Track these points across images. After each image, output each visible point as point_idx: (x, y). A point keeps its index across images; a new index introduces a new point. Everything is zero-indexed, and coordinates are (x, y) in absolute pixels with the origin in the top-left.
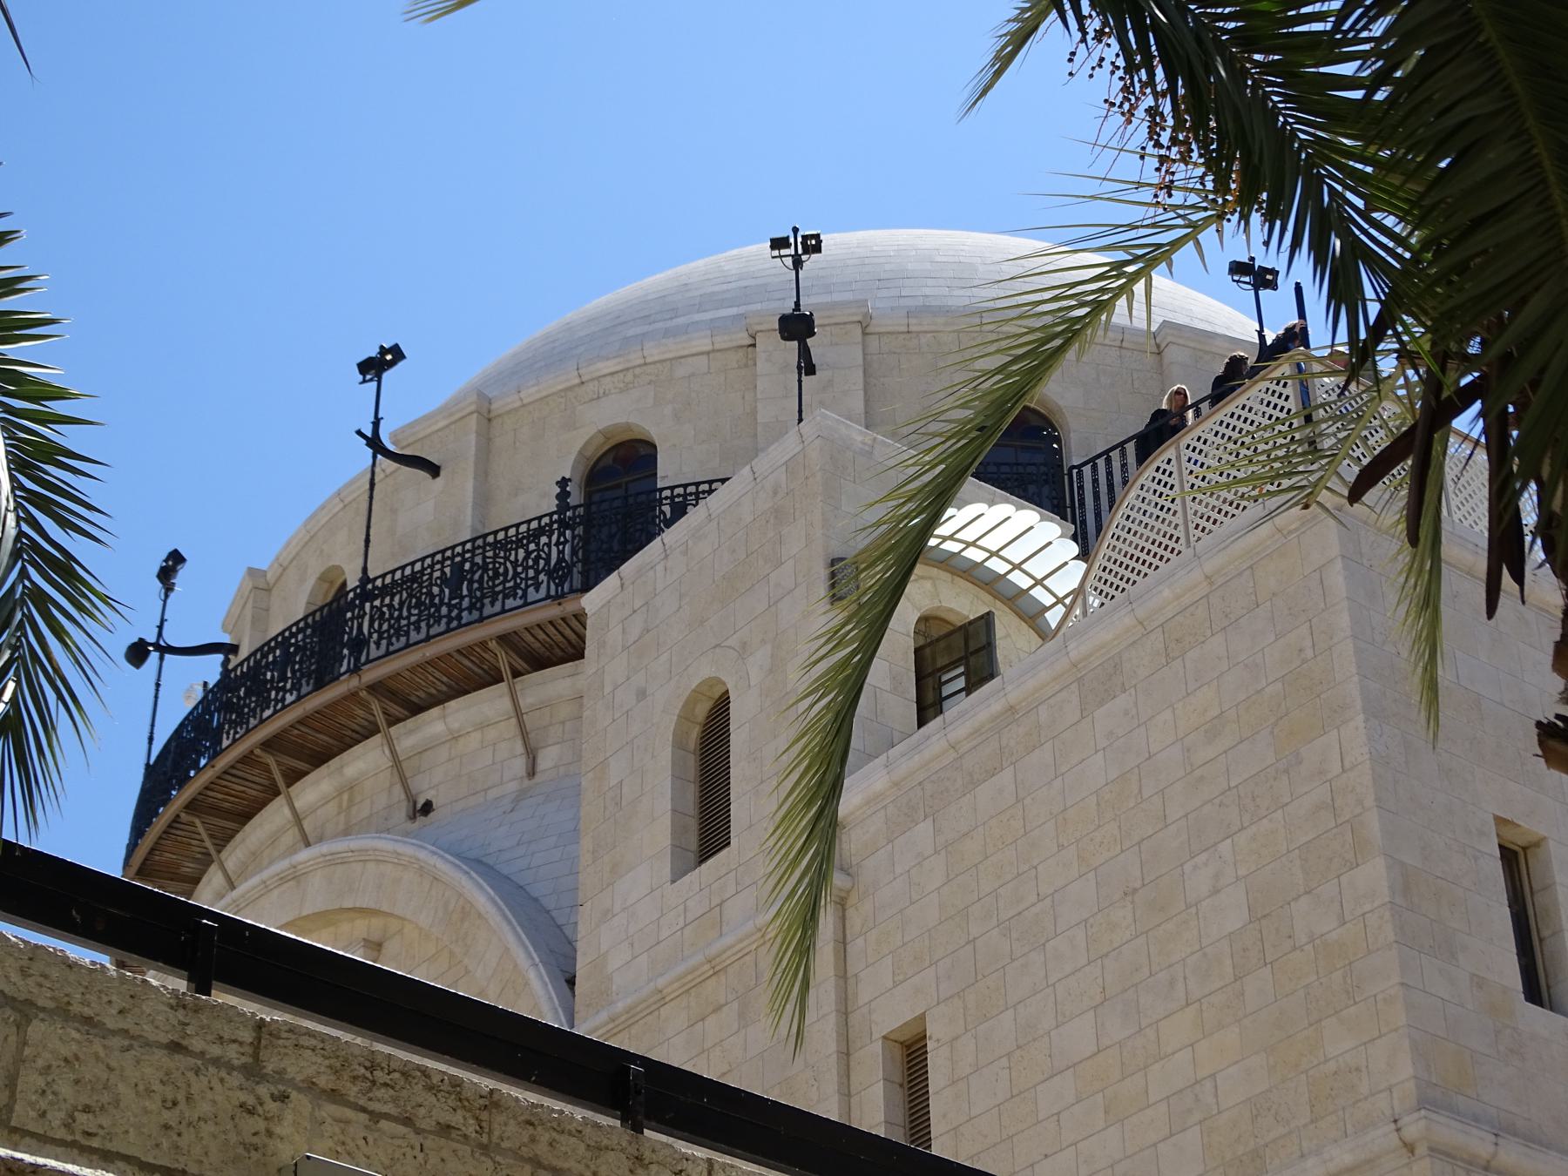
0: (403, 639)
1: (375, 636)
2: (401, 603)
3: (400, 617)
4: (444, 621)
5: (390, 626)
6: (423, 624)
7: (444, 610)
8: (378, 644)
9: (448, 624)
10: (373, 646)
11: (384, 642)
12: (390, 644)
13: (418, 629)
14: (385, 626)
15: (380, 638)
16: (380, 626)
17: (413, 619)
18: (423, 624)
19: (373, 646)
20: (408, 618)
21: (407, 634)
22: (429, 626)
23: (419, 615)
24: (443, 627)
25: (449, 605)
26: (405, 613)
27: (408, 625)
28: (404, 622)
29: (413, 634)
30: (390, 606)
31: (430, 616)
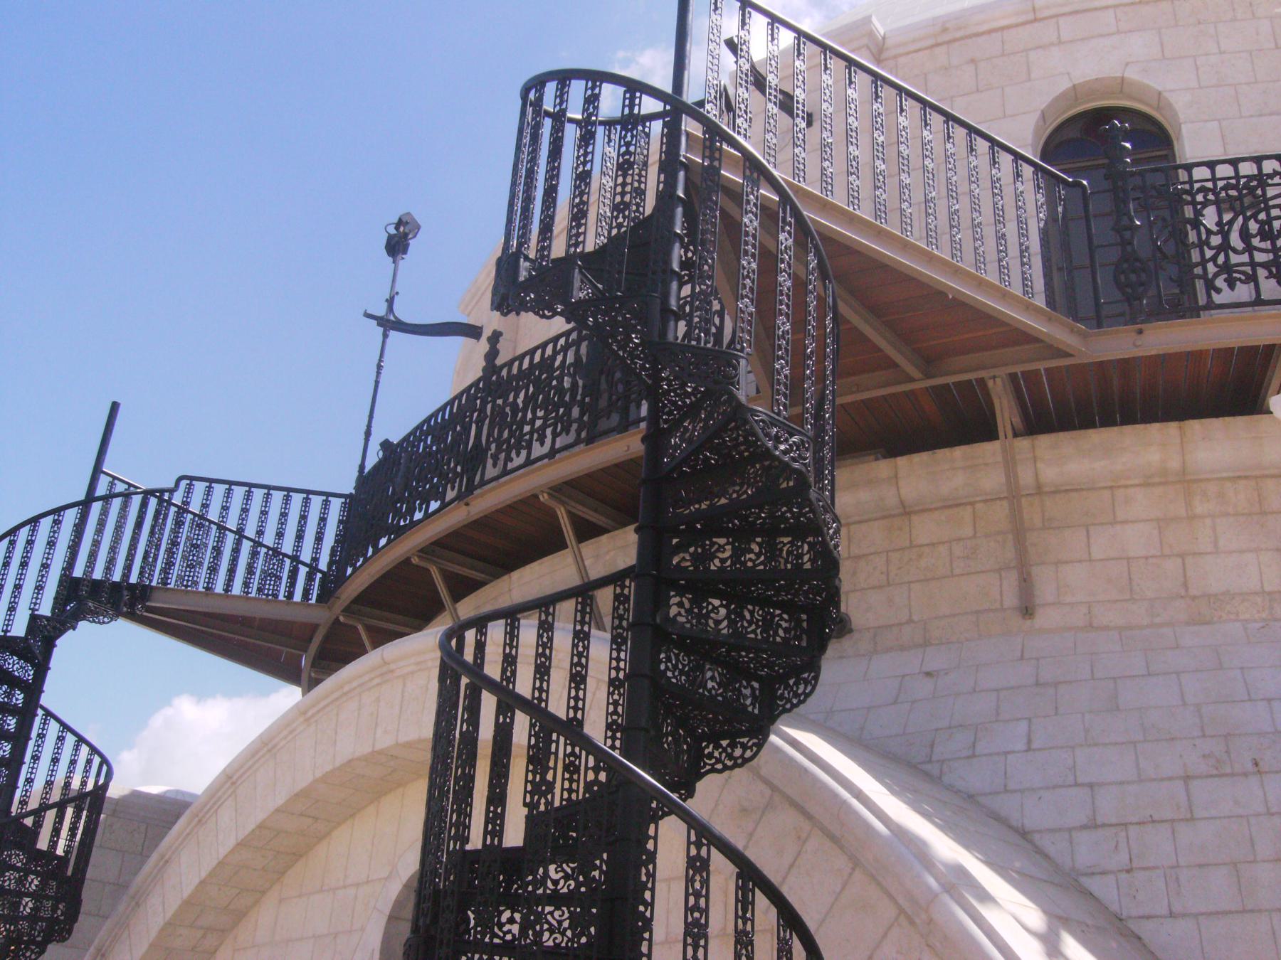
0: (524, 453)
1: (493, 446)
2: (526, 403)
3: (523, 421)
4: (575, 426)
5: (511, 434)
6: (549, 431)
7: (576, 412)
8: (495, 458)
9: (578, 432)
10: (490, 461)
11: (503, 456)
12: (509, 459)
13: (542, 441)
14: (506, 434)
16: (500, 433)
17: (538, 423)
18: (549, 431)
19: (490, 461)
20: (532, 422)
21: (529, 448)
22: (555, 435)
23: (545, 418)
24: (571, 438)
26: (529, 416)
27: (531, 433)
28: (527, 428)
29: (536, 445)
30: (514, 405)
31: (558, 419)
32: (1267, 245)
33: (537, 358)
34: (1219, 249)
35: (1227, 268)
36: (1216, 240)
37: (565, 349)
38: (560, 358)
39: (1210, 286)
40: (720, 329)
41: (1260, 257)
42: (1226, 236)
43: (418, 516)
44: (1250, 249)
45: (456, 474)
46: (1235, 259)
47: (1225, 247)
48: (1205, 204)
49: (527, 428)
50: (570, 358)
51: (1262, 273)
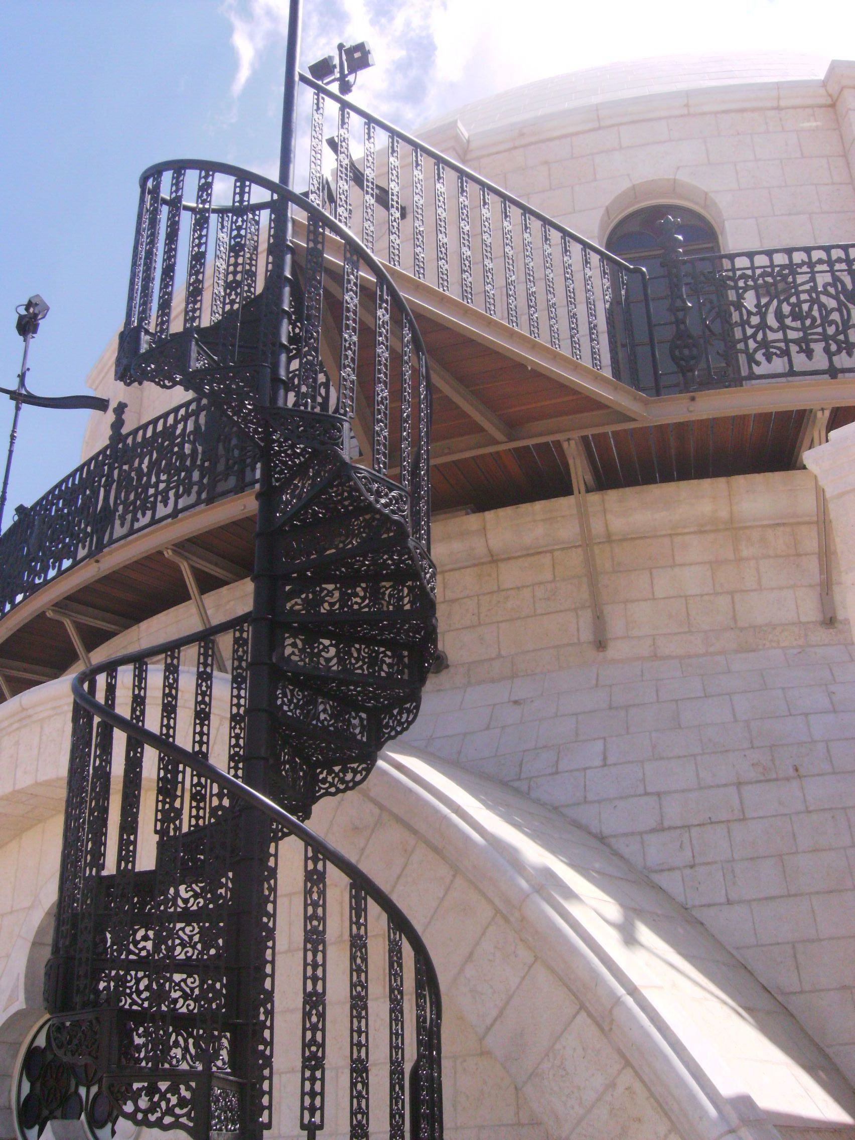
0: (149, 513)
1: (121, 508)
3: (148, 485)
4: (195, 488)
6: (171, 494)
7: (196, 475)
9: (199, 493)
10: (118, 522)
11: (129, 517)
12: (135, 519)
13: (165, 502)
14: (132, 497)
15: (126, 511)
17: (162, 486)
18: (171, 494)
19: (118, 522)
21: (154, 509)
22: (178, 496)
23: (168, 481)
24: (193, 498)
25: (201, 468)
26: (154, 479)
28: (151, 491)
29: (160, 506)
31: (179, 482)
32: (798, 324)
33: (160, 427)
34: (758, 328)
35: (765, 344)
36: (755, 320)
37: (185, 419)
38: (180, 427)
39: (751, 360)
40: (326, 399)
41: (792, 335)
42: (763, 317)
43: (52, 573)
44: (783, 328)
45: (87, 535)
46: (771, 336)
47: (763, 326)
48: (746, 289)
49: (151, 491)
50: (190, 426)
51: (794, 348)
